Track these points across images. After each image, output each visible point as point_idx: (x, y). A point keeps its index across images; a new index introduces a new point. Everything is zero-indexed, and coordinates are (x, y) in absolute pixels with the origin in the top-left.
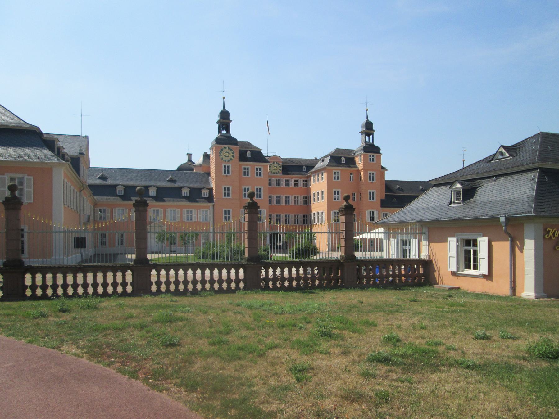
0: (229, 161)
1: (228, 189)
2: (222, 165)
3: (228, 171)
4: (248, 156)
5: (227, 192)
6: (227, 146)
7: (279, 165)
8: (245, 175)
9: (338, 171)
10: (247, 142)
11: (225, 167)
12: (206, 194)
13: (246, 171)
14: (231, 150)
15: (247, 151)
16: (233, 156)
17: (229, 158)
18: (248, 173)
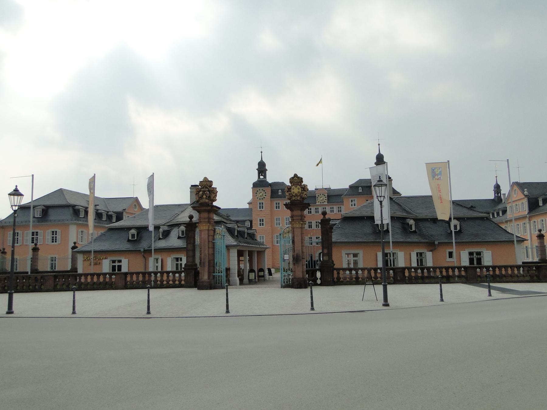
0: (262, 199)
1: (263, 220)
2: (257, 202)
3: (262, 206)
4: (279, 194)
5: (262, 222)
6: (261, 189)
7: (325, 195)
8: (277, 208)
9: (354, 199)
10: (283, 182)
11: (260, 204)
12: (249, 225)
13: (278, 205)
14: (264, 191)
15: (279, 189)
16: (265, 195)
17: (262, 197)
18: (279, 206)
